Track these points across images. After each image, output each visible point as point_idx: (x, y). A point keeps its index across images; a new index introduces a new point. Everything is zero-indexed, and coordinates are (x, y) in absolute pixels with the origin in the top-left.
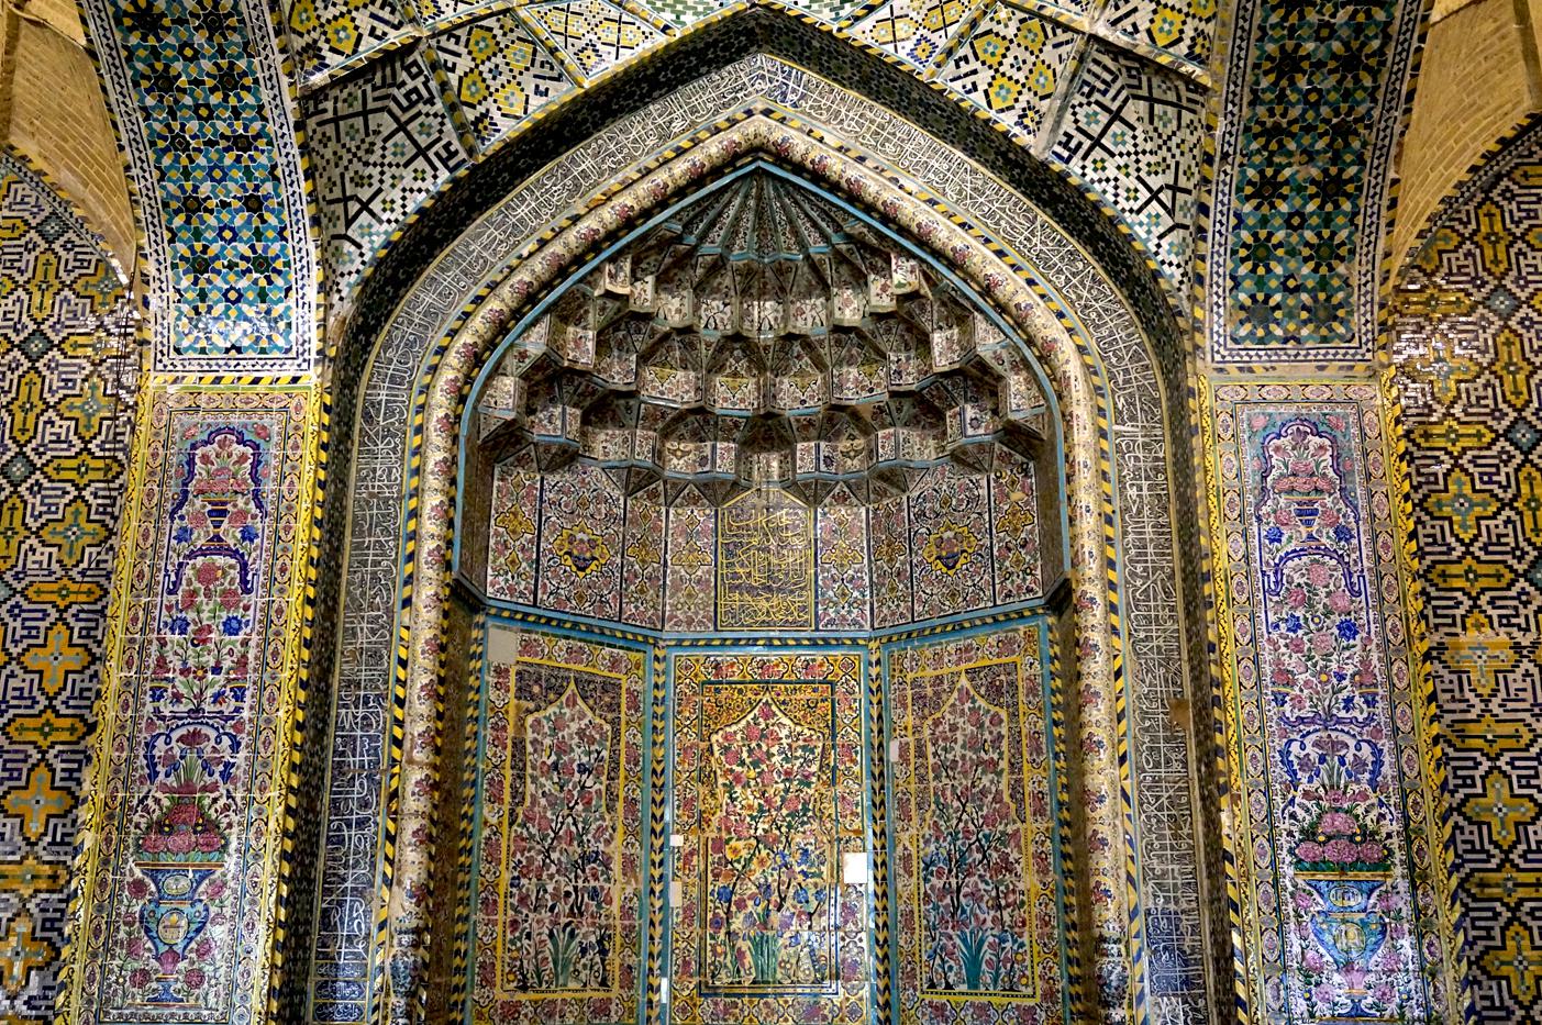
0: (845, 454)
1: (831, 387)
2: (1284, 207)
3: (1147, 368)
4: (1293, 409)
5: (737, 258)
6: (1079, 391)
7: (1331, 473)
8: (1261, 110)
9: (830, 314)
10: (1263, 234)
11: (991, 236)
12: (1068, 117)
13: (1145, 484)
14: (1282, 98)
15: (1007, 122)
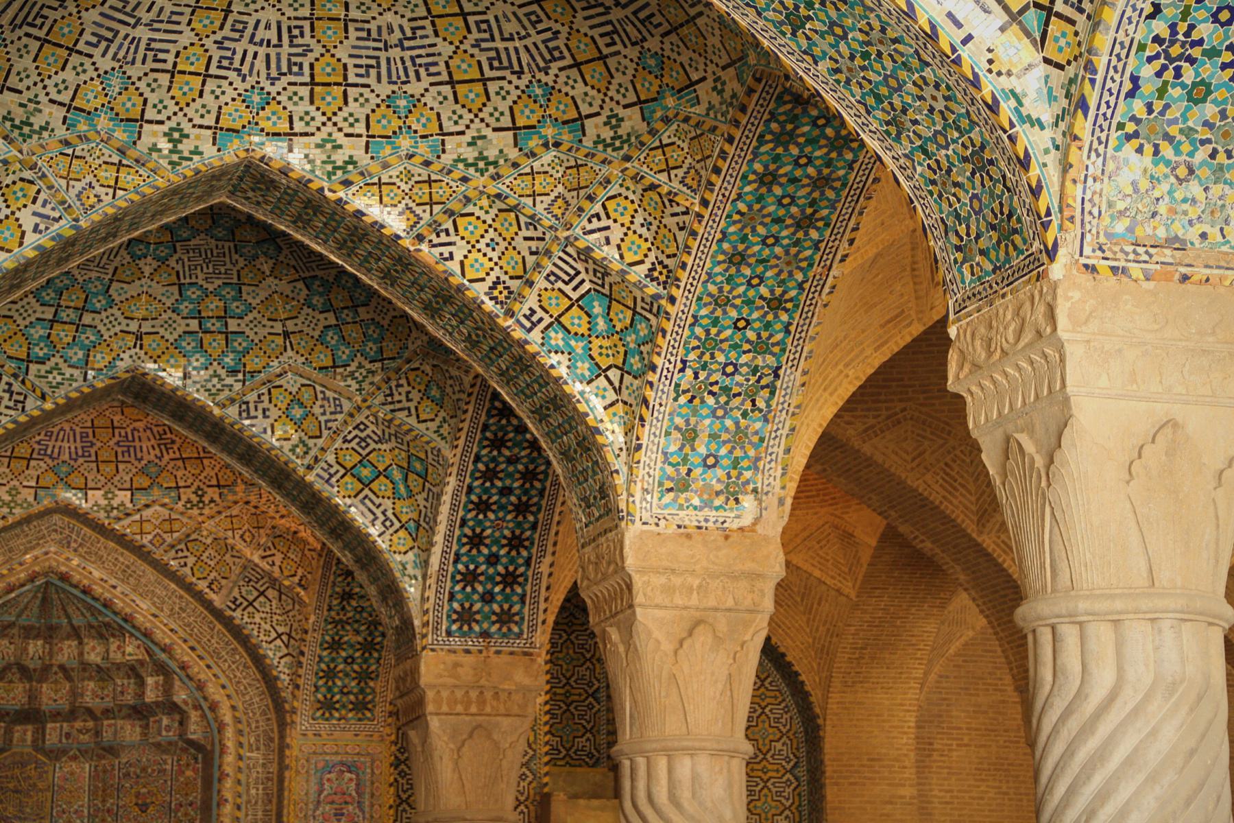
0: (80, 731)
1: (74, 694)
2: (344, 654)
3: (268, 719)
4: (339, 758)
5: (23, 621)
6: (229, 733)
7: (354, 793)
8: (333, 613)
9: (81, 654)
10: (332, 666)
11: (188, 637)
12: (236, 589)
13: (261, 787)
14: (343, 608)
15: (202, 585)
